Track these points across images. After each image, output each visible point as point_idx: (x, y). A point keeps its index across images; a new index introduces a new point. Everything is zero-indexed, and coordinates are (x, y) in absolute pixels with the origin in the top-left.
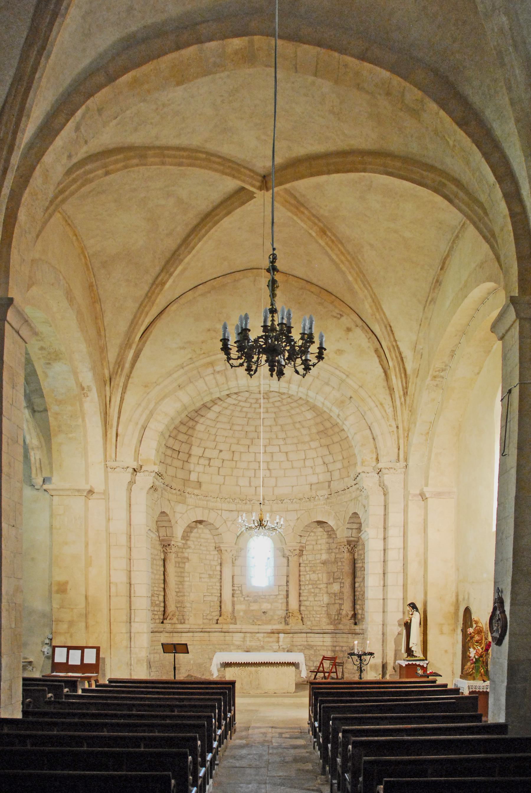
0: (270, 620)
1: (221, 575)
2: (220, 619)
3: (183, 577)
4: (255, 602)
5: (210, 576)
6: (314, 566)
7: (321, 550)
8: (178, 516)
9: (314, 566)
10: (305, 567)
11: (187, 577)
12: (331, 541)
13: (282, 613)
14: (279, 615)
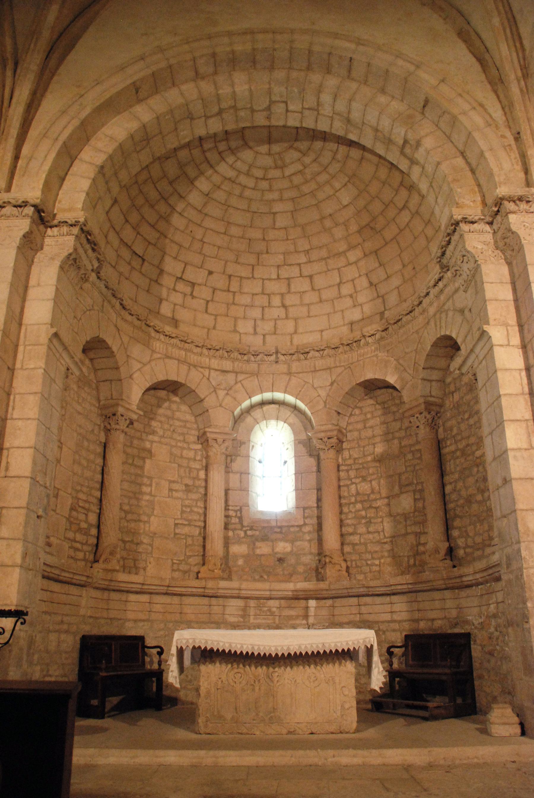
0: (291, 575)
1: (206, 488)
2: (203, 569)
3: (140, 485)
4: (265, 539)
5: (188, 489)
6: (364, 468)
7: (374, 436)
8: (136, 366)
9: (364, 468)
10: (348, 471)
11: (147, 485)
12: (390, 418)
13: (309, 560)
14: (306, 565)
